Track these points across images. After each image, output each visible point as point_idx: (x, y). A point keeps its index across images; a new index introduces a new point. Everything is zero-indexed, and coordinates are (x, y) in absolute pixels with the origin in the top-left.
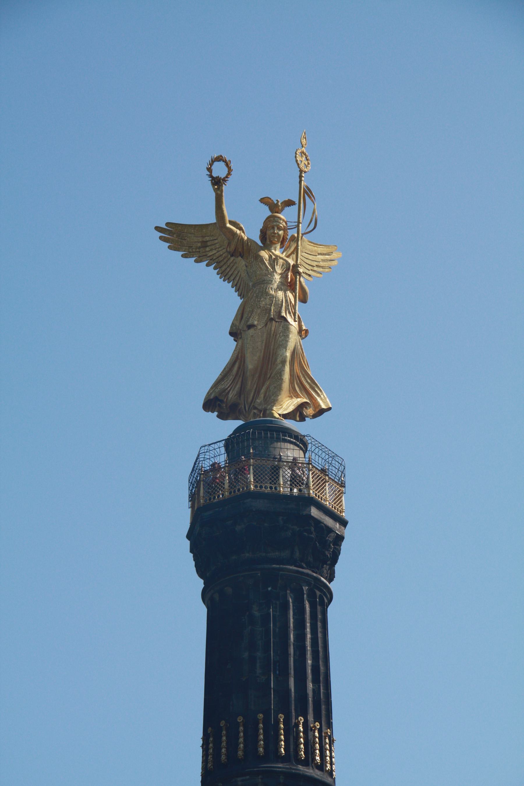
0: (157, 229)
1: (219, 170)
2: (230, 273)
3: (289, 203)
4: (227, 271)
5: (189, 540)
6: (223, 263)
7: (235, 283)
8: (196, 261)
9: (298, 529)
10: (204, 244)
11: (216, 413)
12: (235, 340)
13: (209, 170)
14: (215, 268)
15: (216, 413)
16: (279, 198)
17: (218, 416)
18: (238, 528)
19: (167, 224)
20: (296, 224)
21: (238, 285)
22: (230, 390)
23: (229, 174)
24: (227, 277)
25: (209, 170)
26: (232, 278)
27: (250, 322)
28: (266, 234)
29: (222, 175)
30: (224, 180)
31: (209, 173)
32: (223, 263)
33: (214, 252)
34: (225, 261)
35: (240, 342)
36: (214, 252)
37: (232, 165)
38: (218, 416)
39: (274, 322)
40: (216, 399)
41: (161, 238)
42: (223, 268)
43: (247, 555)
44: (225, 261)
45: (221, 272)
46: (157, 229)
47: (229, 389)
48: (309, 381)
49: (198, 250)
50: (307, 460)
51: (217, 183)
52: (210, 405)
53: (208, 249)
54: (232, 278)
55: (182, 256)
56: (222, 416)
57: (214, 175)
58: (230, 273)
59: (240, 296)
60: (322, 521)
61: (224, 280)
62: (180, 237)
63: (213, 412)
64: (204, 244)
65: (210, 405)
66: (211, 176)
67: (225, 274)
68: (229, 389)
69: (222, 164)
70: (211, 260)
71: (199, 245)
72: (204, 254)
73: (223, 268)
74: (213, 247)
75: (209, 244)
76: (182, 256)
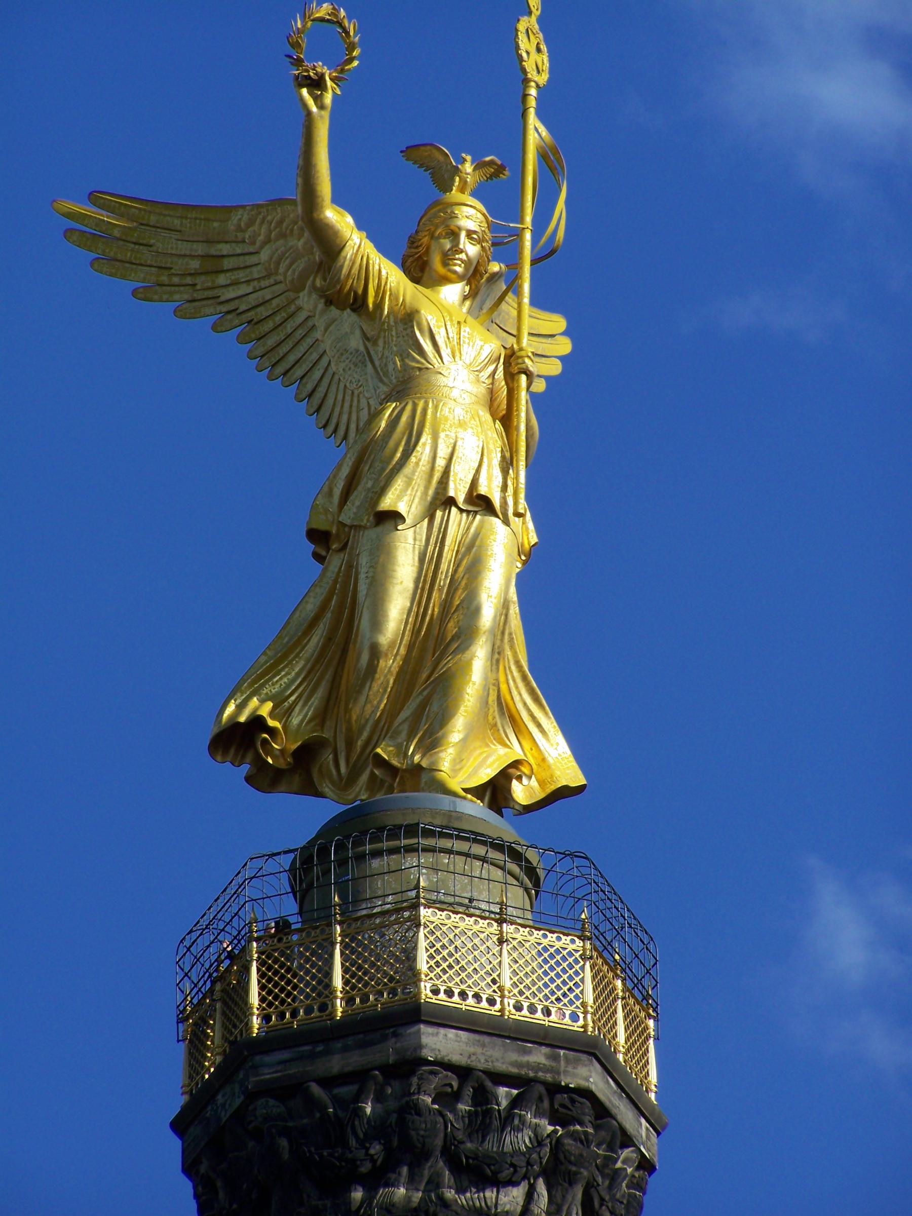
2: (292, 358)
6: (270, 325)
7: (309, 387)
9: (550, 1128)
10: (213, 265)
14: (242, 339)
15: (245, 768)
17: (248, 779)
22: (295, 702)
24: (280, 369)
26: (299, 372)
32: (270, 325)
33: (244, 289)
34: (278, 319)
35: (336, 562)
36: (244, 289)
38: (248, 779)
39: (454, 509)
42: (271, 341)
44: (278, 319)
45: (260, 351)
47: (293, 698)
49: (189, 280)
53: (222, 279)
54: (299, 372)
56: (265, 778)
58: (292, 358)
60: (614, 1111)
64: (213, 265)
67: (274, 360)
68: (293, 698)
70: (229, 312)
71: (195, 264)
72: (210, 293)
73: (271, 341)
74: (241, 275)
75: (227, 264)
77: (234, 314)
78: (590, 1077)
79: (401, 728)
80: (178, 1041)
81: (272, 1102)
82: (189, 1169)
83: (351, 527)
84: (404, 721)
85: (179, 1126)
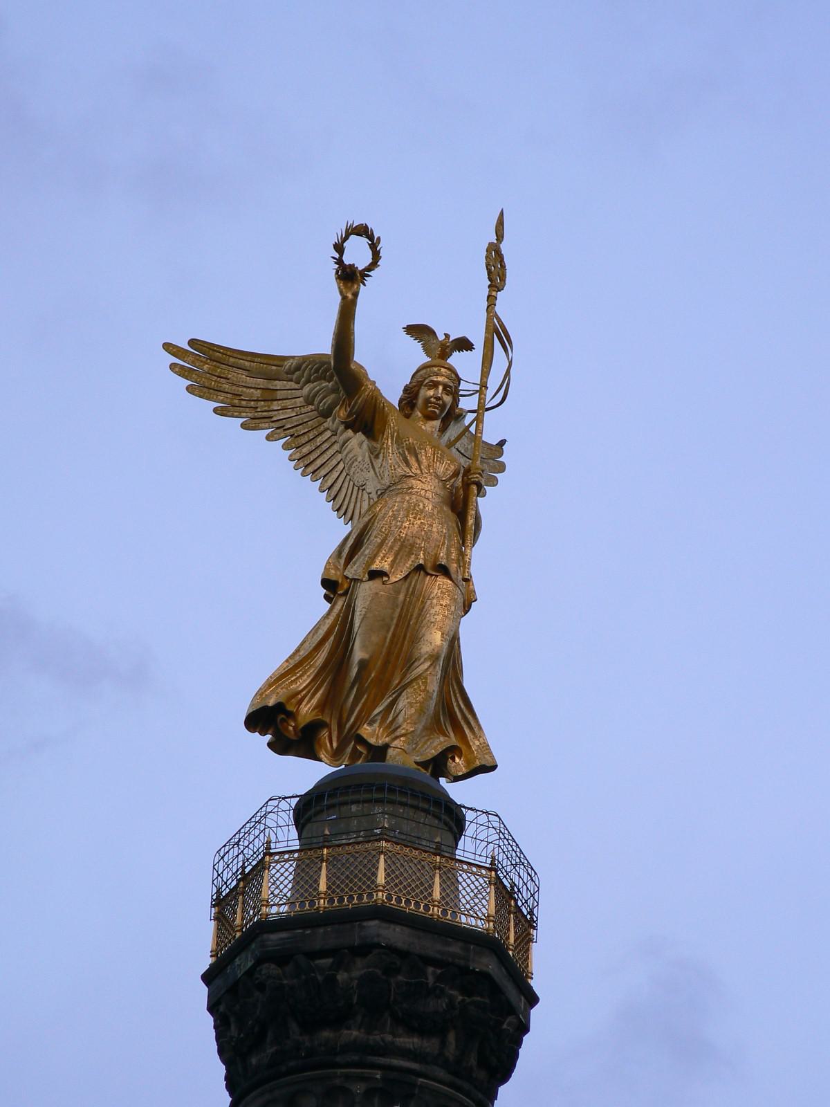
0: (168, 347)
1: (357, 252)
2: (319, 462)
3: (464, 344)
4: (312, 457)
5: (207, 985)
6: (305, 439)
7: (329, 483)
8: (244, 426)
9: (460, 998)
11: (268, 737)
12: (327, 597)
13: (339, 248)
14: (286, 447)
15: (268, 737)
16: (445, 328)
17: (270, 745)
18: (342, 976)
19: (192, 342)
20: (478, 388)
21: (336, 488)
23: (374, 264)
24: (310, 469)
25: (339, 248)
26: (323, 472)
27: (375, 566)
28: (416, 396)
29: (361, 265)
30: (364, 274)
31: (337, 256)
32: (305, 439)
33: (290, 413)
34: (311, 435)
35: (340, 603)
36: (290, 413)
37: (383, 247)
38: (270, 745)
39: (422, 572)
40: (280, 707)
41: (173, 367)
42: (305, 450)
43: (355, 1033)
44: (311, 435)
45: (298, 456)
46: (168, 347)
47: (304, 692)
48: (462, 706)
50: (489, 861)
51: (349, 277)
52: (258, 720)
53: (275, 406)
54: (323, 472)
55: (216, 410)
56: (281, 746)
57: (347, 260)
58: (319, 462)
59: (338, 510)
61: (501, 468)
62: (214, 371)
63: (263, 733)
65: (258, 720)
66: (339, 262)
67: (306, 463)
68: (304, 692)
69: (364, 241)
70: (278, 428)
71: (258, 393)
72: (265, 414)
73: (305, 450)
74: (288, 403)
75: (279, 395)
76: (216, 410)
77: (282, 429)
78: (488, 964)
79: (376, 718)
80: (211, 920)
81: (273, 966)
82: (211, 1009)
83: (352, 580)
84: (379, 713)
85: (207, 978)
